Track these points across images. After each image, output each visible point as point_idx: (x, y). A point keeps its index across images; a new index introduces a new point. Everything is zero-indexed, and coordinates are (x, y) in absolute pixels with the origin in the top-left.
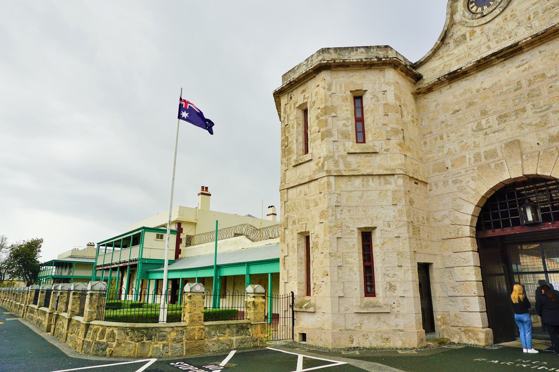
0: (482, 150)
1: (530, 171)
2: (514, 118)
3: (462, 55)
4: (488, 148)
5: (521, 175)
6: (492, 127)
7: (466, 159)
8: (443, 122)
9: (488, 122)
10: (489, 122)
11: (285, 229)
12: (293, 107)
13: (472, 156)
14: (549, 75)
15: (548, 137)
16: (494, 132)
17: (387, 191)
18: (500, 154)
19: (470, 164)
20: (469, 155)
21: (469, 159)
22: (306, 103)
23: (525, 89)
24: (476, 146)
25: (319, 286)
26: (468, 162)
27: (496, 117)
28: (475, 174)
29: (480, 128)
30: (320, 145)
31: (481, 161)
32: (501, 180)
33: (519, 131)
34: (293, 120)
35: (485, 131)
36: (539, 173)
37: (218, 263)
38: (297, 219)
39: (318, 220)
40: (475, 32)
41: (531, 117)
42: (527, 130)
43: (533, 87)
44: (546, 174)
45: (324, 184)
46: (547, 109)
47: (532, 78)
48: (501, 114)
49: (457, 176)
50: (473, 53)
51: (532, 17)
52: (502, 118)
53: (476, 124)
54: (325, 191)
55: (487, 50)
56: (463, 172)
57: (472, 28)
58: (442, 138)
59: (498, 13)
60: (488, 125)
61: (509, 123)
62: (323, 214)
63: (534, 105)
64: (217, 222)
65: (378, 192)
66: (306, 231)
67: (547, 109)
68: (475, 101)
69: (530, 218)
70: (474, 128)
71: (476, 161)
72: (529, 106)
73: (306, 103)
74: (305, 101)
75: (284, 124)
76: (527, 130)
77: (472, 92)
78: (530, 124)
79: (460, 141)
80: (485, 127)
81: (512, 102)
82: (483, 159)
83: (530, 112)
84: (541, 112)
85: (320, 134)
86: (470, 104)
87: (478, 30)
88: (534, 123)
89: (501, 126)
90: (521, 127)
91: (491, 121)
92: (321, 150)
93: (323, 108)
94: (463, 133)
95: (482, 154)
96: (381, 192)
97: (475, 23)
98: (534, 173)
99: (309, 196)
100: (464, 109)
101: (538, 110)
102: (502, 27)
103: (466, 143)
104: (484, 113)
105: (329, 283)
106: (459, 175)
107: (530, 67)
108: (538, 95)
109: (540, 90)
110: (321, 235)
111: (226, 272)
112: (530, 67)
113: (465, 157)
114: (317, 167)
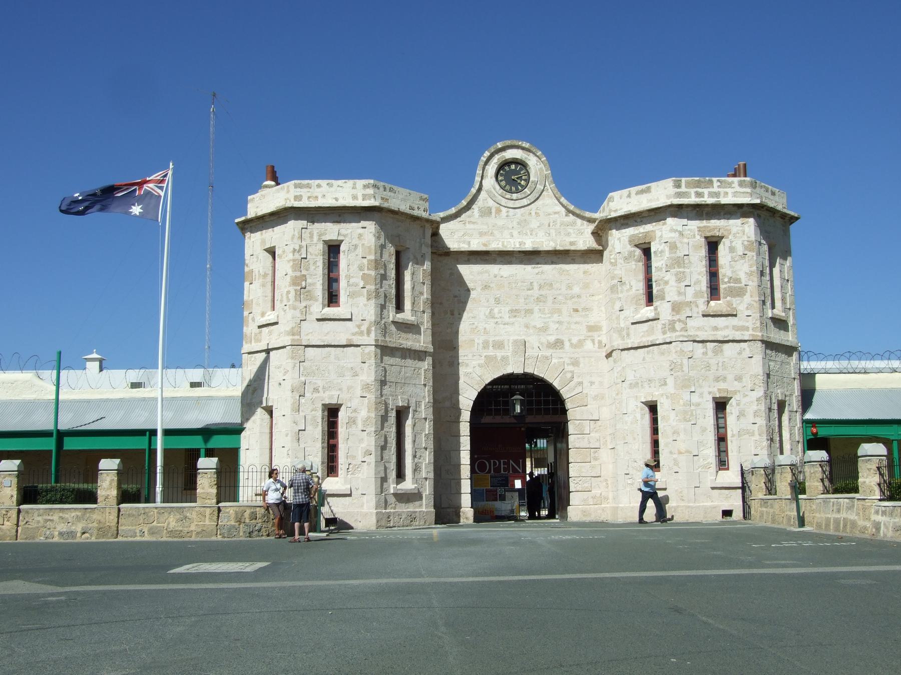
0: (491, 339)
1: (529, 370)
2: (523, 316)
3: (486, 231)
4: (497, 338)
5: (523, 372)
6: (503, 318)
7: (474, 344)
8: (456, 297)
9: (500, 312)
10: (501, 313)
11: (300, 396)
12: (315, 238)
13: (481, 341)
14: (554, 286)
15: (546, 343)
16: (504, 324)
17: (420, 368)
18: (506, 347)
19: (477, 350)
20: (479, 340)
21: (478, 344)
22: (342, 241)
23: (536, 292)
24: (486, 331)
25: (357, 466)
26: (476, 347)
27: (508, 310)
28: (482, 362)
29: (491, 315)
30: (365, 305)
31: (489, 349)
32: (505, 372)
33: (525, 330)
34: (316, 255)
35: (496, 320)
36: (535, 373)
37: (62, 427)
38: (321, 387)
39: (359, 393)
40: (501, 211)
41: (537, 320)
42: (531, 331)
43: (543, 293)
44: (540, 376)
45: (369, 353)
46: (549, 318)
47: (543, 284)
48: (513, 308)
49: (464, 358)
50: (496, 232)
51: (551, 225)
52: (514, 312)
53: (489, 311)
54: (370, 361)
55: (509, 237)
56: (470, 356)
57: (499, 205)
58: (452, 314)
59: (526, 204)
60: (500, 315)
61: (519, 319)
62: (366, 387)
63: (540, 310)
64: (60, 353)
65: (413, 369)
66: (338, 403)
67: (549, 318)
68: (491, 285)
69: (518, 409)
70: (487, 314)
71: (484, 348)
72: (536, 309)
73: (342, 241)
74: (340, 238)
75: (300, 255)
76: (531, 331)
77: (489, 276)
78: (535, 327)
79: (471, 323)
80: (496, 316)
81: (523, 300)
82: (491, 348)
83: (536, 314)
84: (544, 318)
85: (365, 290)
86: (486, 286)
87: (504, 210)
88: (538, 326)
89: (511, 320)
90: (527, 326)
91: (503, 312)
92: (367, 312)
93: (371, 261)
94: (475, 316)
95: (491, 342)
96: (415, 370)
97: (503, 202)
98: (532, 372)
99: (343, 362)
100: (479, 290)
101: (542, 316)
102: (525, 220)
103: (477, 327)
104: (498, 301)
105: (373, 464)
106: (466, 358)
107: (542, 273)
108: (544, 302)
109: (546, 298)
110: (361, 410)
111: (70, 444)
112: (542, 273)
113: (474, 341)
114: (357, 330)
